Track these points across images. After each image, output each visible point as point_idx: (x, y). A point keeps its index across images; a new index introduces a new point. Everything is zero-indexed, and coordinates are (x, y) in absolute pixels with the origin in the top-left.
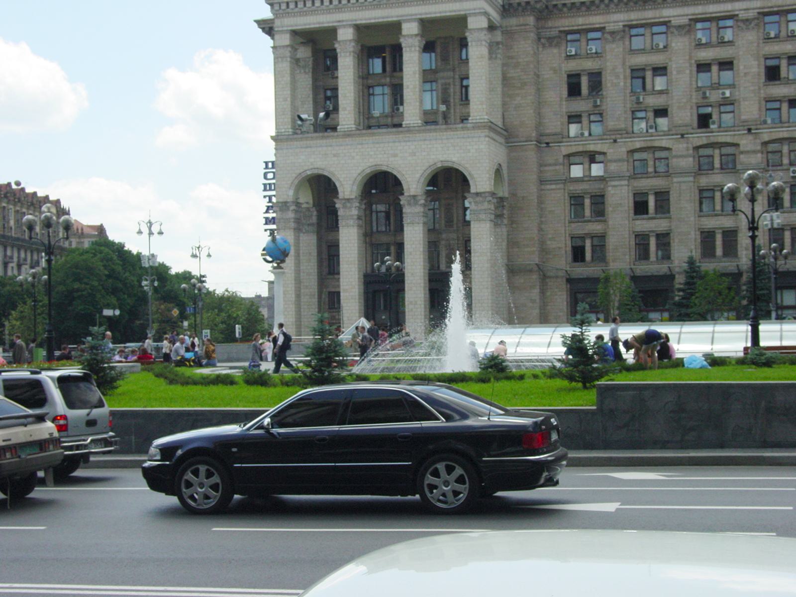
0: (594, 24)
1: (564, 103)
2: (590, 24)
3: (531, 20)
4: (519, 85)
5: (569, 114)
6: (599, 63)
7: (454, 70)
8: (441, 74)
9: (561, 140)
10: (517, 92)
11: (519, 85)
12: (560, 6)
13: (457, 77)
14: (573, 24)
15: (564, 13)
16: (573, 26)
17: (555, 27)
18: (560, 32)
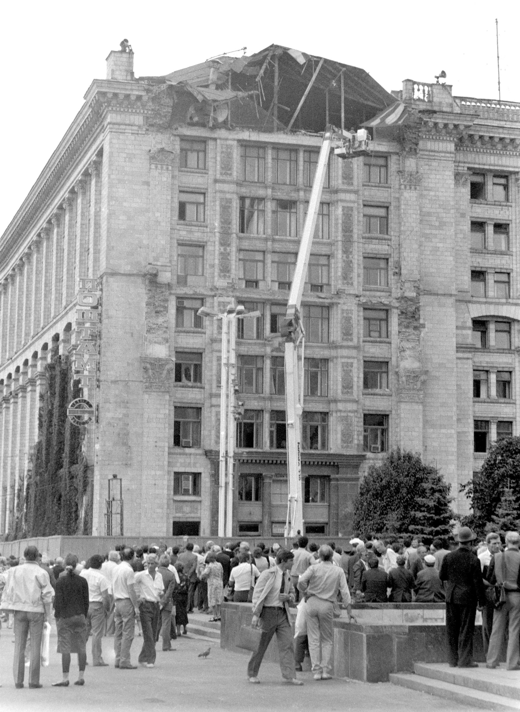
0: (507, 166)
1: (469, 254)
2: (502, 166)
3: (451, 147)
4: (437, 224)
5: (474, 269)
6: (507, 213)
7: (356, 192)
8: (342, 196)
9: (471, 299)
10: (434, 232)
11: (437, 224)
12: (476, 138)
13: (361, 202)
14: (485, 162)
15: (476, 147)
16: (484, 165)
17: (464, 162)
18: (469, 169)
